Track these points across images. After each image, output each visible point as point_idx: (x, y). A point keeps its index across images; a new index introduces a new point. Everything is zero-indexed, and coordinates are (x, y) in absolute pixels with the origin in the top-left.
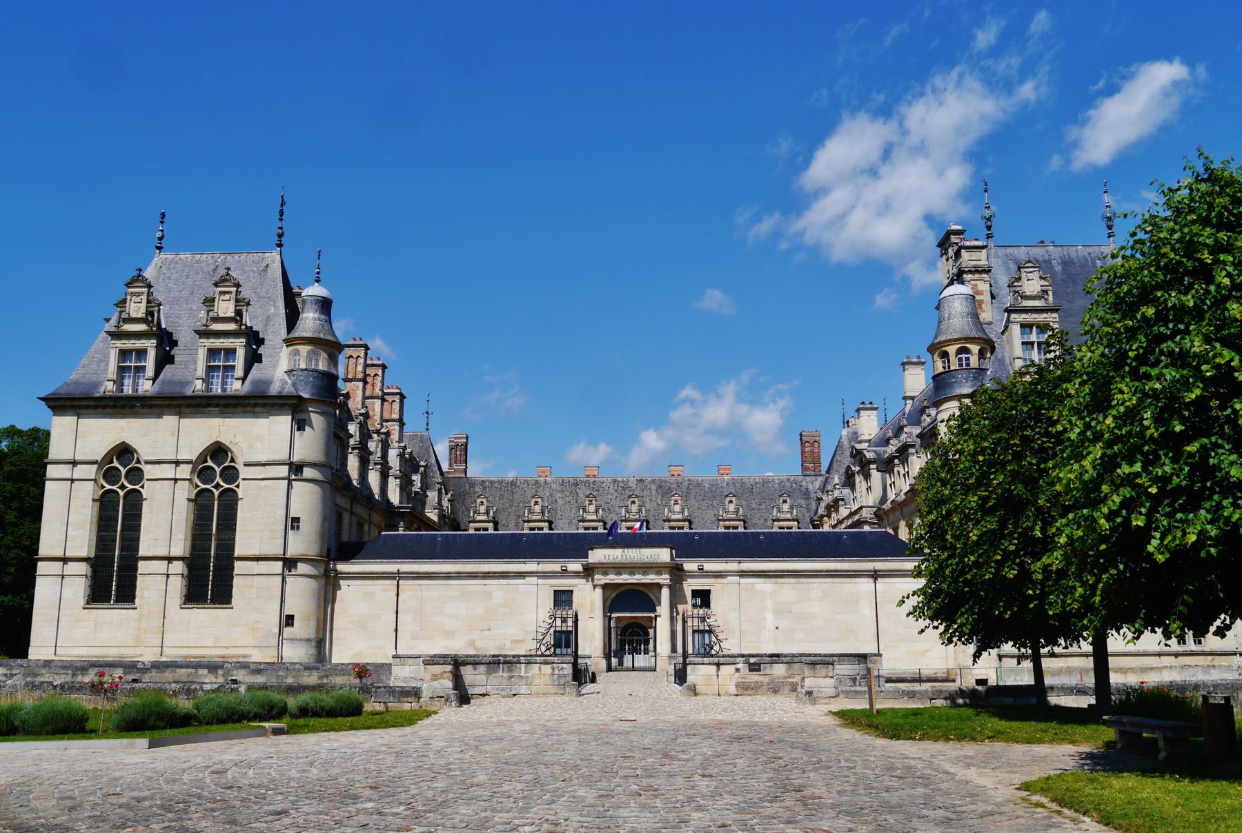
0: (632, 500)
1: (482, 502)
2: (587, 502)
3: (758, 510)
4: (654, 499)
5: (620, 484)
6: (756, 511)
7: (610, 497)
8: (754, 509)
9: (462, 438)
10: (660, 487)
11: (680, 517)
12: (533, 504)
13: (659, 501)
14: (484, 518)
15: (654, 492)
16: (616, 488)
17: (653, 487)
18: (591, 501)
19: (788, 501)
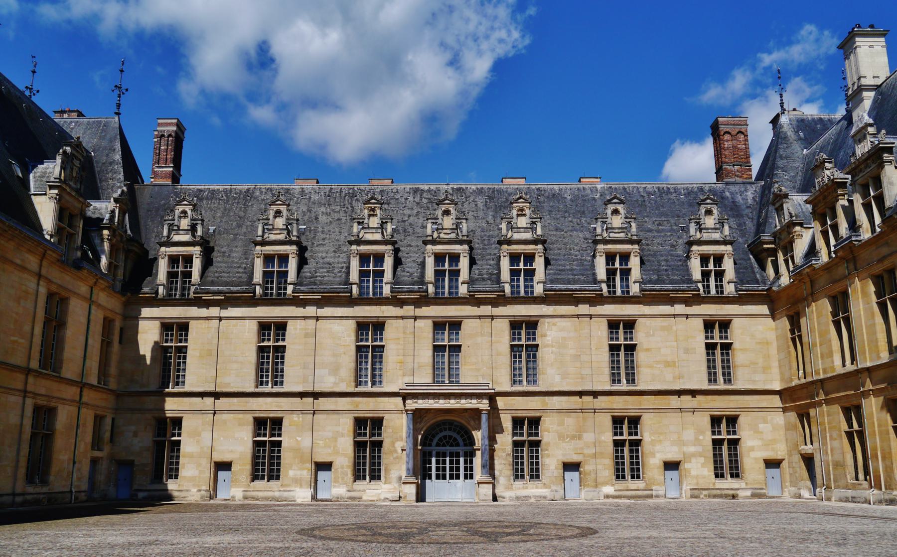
0: (443, 208)
1: (184, 212)
2: (366, 212)
3: (658, 231)
4: (481, 214)
5: (425, 195)
6: (656, 234)
7: (407, 212)
8: (650, 231)
9: (170, 124)
10: (491, 198)
11: (528, 236)
12: (271, 214)
13: (490, 219)
14: (186, 238)
15: (481, 206)
16: (417, 199)
17: (480, 200)
18: (373, 210)
19: (715, 211)
